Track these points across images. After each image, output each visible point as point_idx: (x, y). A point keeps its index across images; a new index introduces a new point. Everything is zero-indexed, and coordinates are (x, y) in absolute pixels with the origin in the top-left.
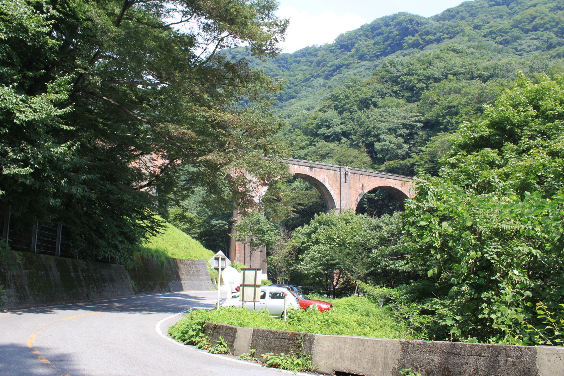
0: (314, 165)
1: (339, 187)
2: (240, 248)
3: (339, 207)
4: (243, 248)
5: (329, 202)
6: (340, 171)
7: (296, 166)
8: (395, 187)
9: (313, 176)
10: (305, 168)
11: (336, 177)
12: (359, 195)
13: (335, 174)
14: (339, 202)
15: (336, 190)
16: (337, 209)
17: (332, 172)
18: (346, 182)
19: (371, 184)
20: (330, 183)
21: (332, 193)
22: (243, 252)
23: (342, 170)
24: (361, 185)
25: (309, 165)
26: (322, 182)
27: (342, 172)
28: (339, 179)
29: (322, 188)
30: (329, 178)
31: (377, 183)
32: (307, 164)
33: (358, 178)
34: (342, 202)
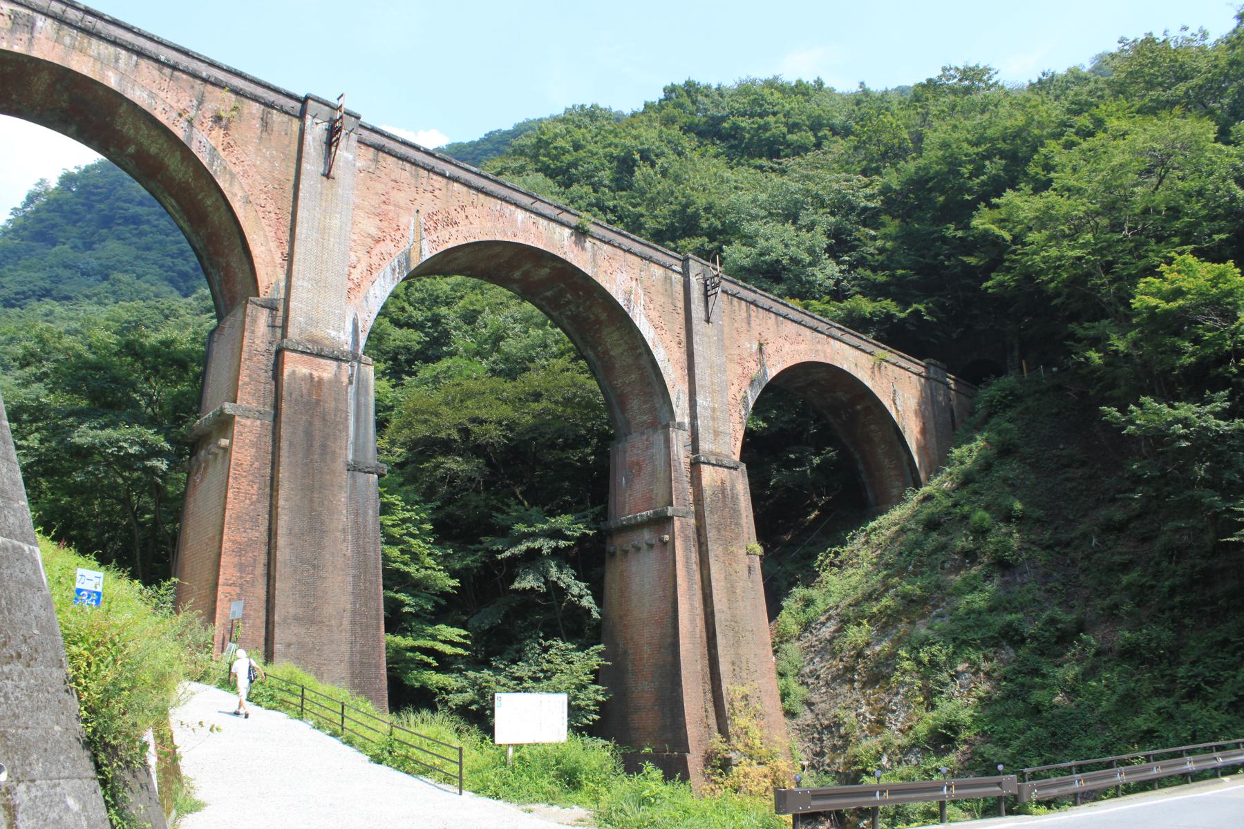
0: (592, 228)
1: (683, 337)
2: (241, 568)
3: (687, 420)
4: (260, 570)
5: (634, 404)
6: (685, 274)
7: (520, 215)
8: (853, 372)
9: (588, 270)
10: (558, 229)
11: (671, 296)
12: (752, 382)
13: (667, 279)
14: (685, 399)
15: (674, 345)
16: (681, 426)
17: (658, 271)
18: (708, 321)
19: (787, 347)
20: (654, 315)
21: (660, 355)
22: (261, 591)
23: (695, 267)
24: (755, 347)
25: (574, 221)
26: (621, 302)
27: (693, 279)
28: (681, 304)
29: (612, 339)
30: (647, 292)
31: (802, 347)
32: (565, 217)
33: (744, 315)
34: (700, 400)
